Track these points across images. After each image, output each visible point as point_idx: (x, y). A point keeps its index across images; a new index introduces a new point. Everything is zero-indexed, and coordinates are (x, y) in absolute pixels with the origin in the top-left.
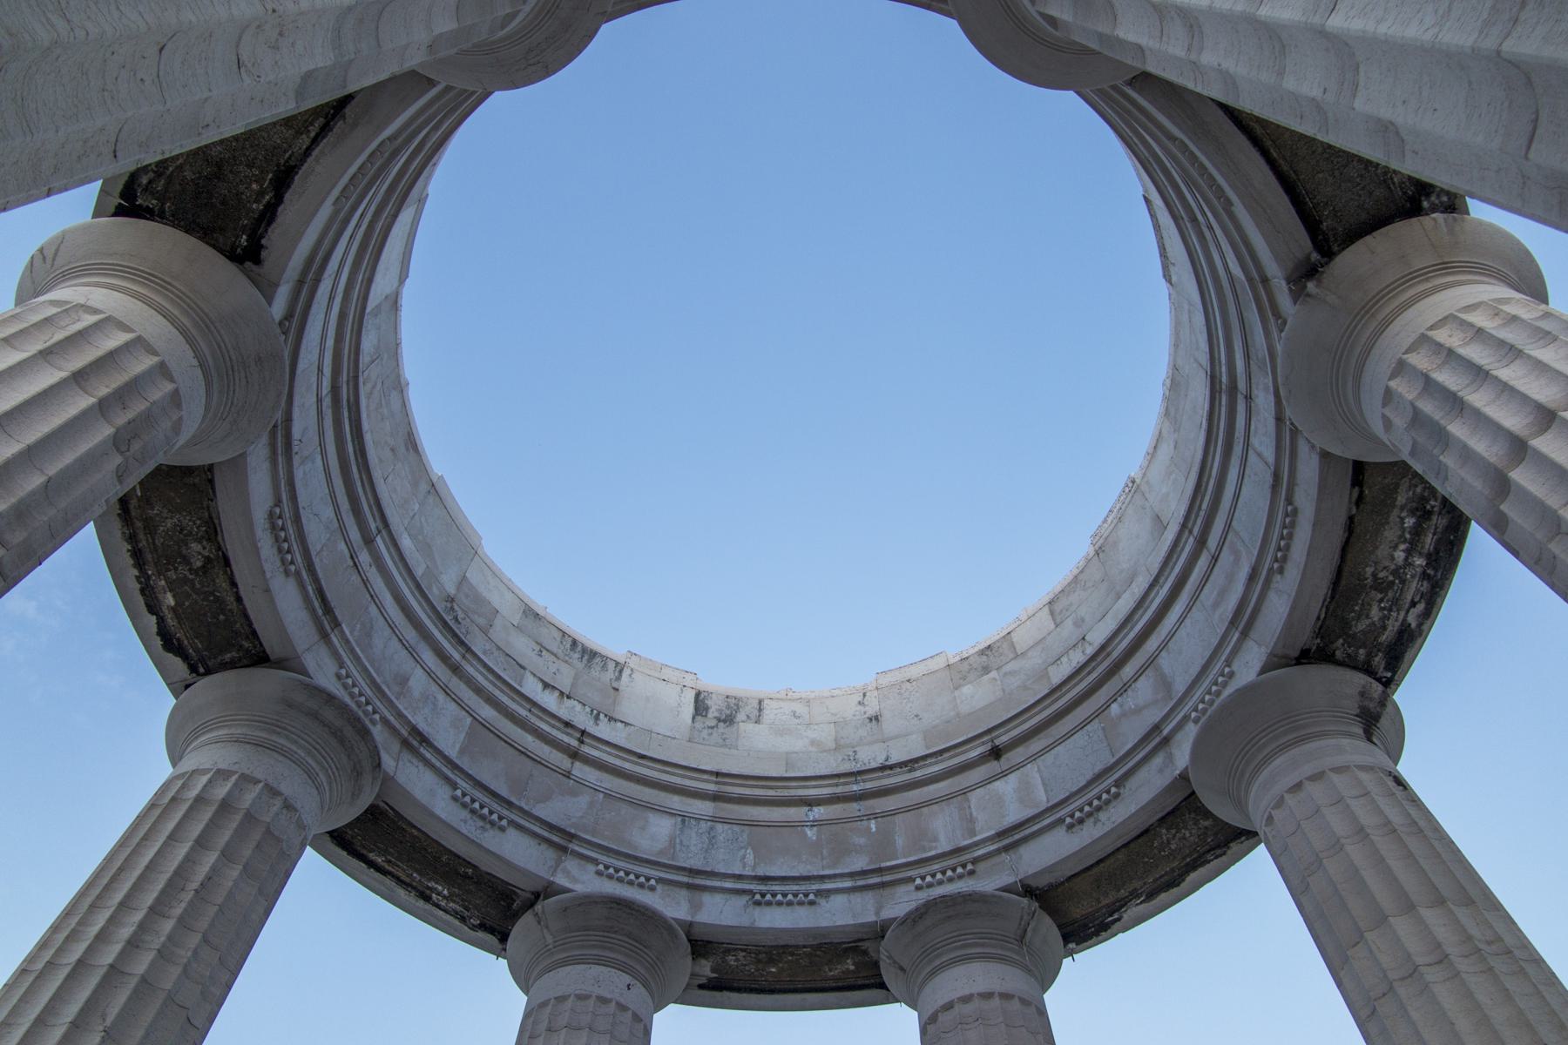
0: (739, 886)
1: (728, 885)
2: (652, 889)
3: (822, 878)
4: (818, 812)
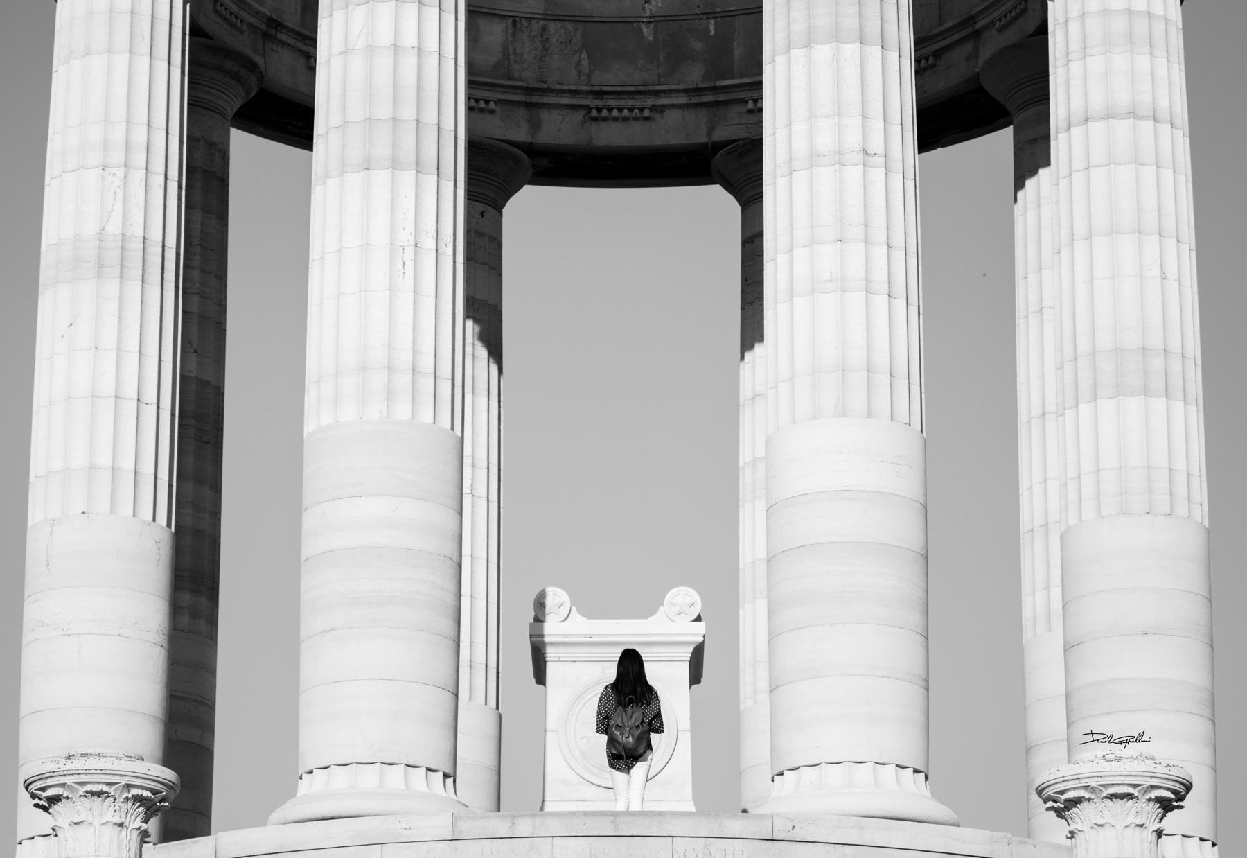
0: (575, 101)
1: (565, 100)
2: (492, 112)
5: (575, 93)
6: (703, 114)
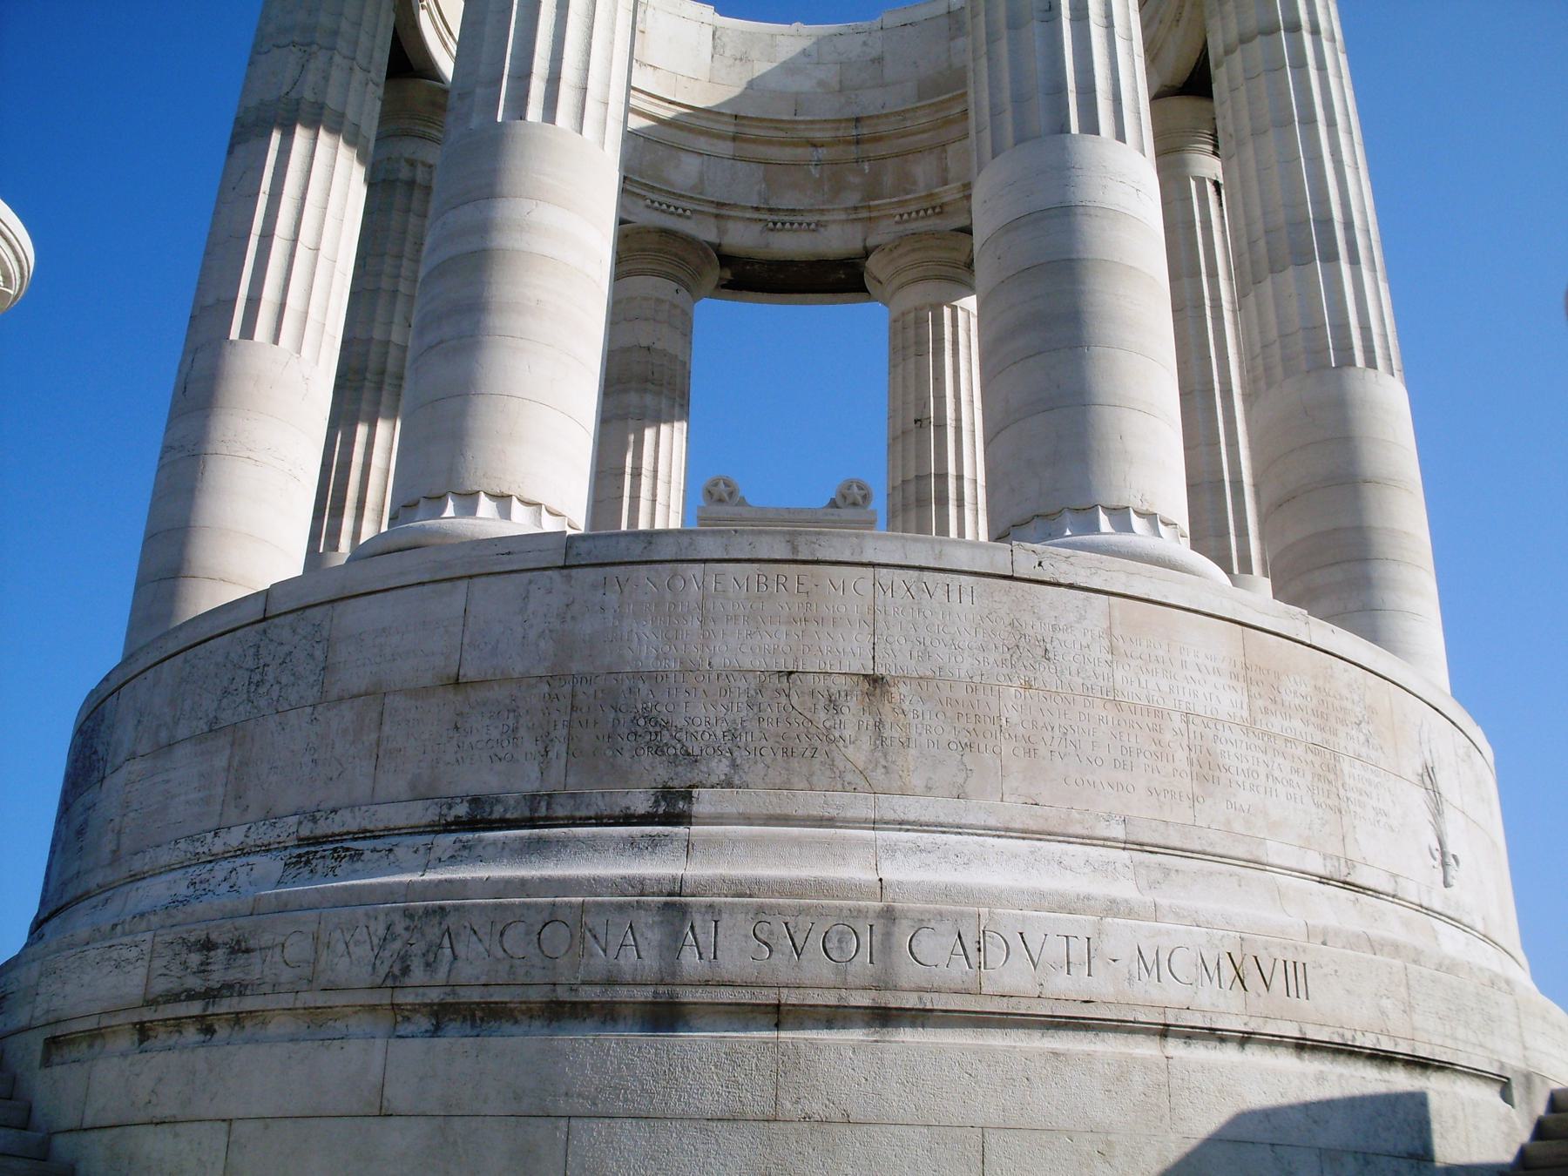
0: (756, 215)
3: (822, 211)
4: (822, 153)
5: (757, 209)
6: (859, 227)
